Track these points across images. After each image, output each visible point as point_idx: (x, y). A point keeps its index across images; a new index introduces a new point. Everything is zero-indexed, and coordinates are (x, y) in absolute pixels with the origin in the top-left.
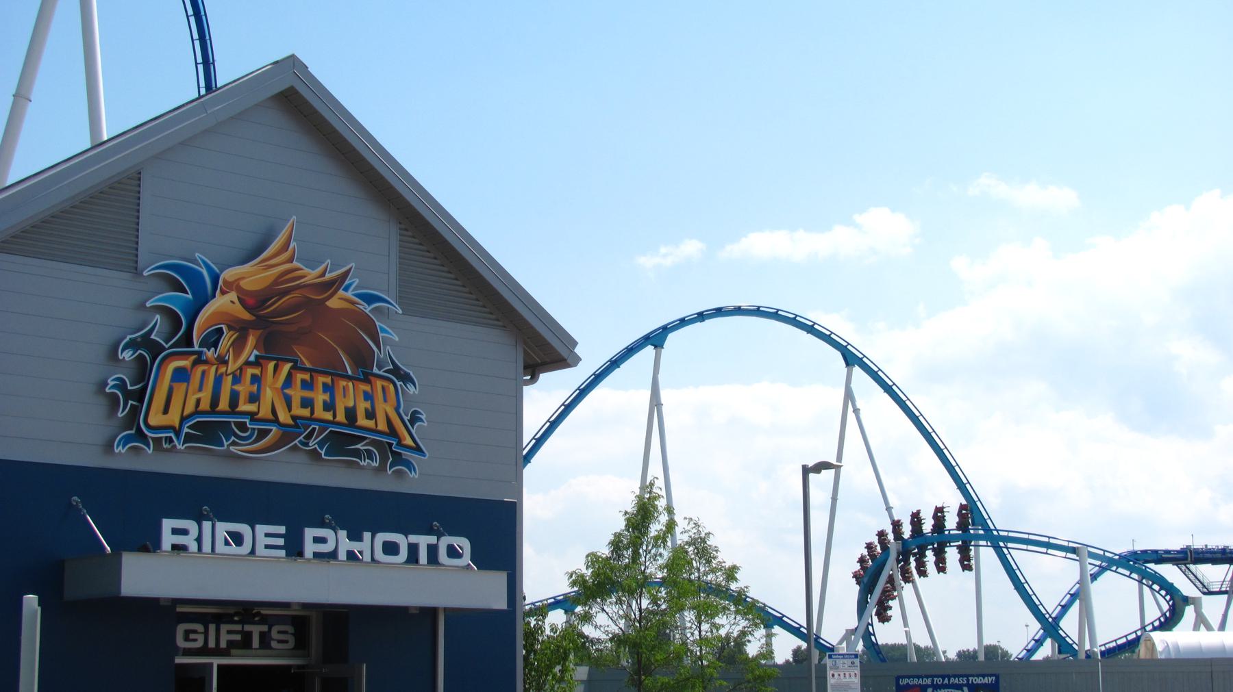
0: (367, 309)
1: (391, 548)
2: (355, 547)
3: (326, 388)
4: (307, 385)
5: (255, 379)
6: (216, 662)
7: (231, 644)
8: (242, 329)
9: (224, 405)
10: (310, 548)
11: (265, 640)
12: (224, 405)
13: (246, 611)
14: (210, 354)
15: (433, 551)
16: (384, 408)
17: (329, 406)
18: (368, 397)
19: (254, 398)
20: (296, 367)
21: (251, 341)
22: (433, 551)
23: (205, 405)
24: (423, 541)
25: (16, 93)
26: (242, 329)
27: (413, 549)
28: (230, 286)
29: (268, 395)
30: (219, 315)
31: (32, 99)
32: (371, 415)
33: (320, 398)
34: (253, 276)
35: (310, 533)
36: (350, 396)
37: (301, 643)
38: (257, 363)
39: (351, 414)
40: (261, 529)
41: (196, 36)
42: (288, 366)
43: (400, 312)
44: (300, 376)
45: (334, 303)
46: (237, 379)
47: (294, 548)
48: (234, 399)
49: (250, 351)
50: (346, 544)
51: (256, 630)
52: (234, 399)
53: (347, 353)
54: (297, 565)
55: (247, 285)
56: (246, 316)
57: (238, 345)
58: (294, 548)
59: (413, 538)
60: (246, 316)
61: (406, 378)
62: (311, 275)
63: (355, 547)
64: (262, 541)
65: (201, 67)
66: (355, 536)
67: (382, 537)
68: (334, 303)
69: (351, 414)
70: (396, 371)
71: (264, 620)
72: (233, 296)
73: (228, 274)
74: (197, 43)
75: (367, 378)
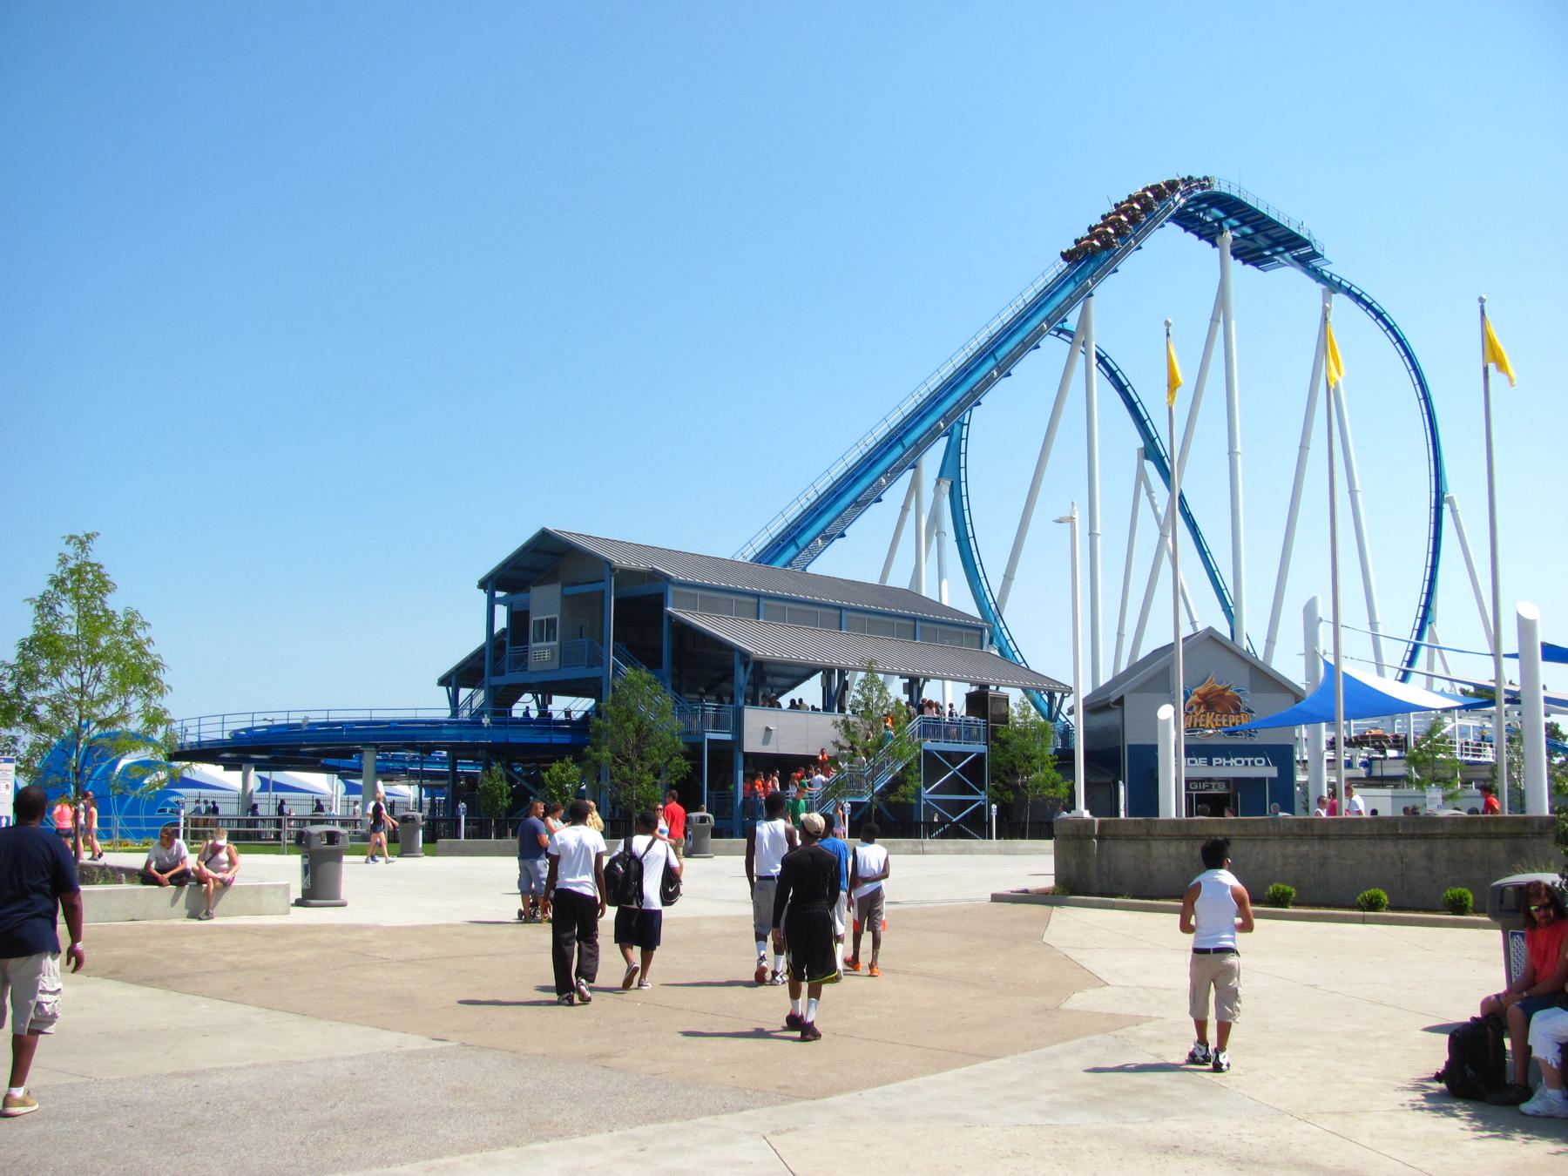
0: (1237, 694)
1: (1239, 762)
2: (1228, 762)
3: (1226, 718)
4: (1219, 717)
5: (1204, 718)
6: (1194, 793)
7: (1206, 788)
8: (1199, 705)
9: (1195, 725)
10: (1214, 763)
11: (1216, 786)
12: (1195, 725)
13: (1209, 780)
14: (1190, 712)
15: (1253, 763)
16: (1245, 722)
17: (1227, 723)
18: (1239, 719)
19: (1204, 723)
20: (1217, 713)
21: (1202, 707)
22: (1253, 763)
23: (1190, 726)
24: (1249, 760)
25: (1301, 444)
26: (1199, 705)
27: (1246, 763)
28: (1195, 693)
29: (1208, 721)
30: (1193, 702)
31: (1311, 446)
32: (1240, 723)
33: (1224, 721)
34: (1202, 690)
35: (1214, 759)
36: (1233, 719)
37: (1228, 787)
38: (1204, 713)
39: (1234, 724)
40: (1200, 759)
41: (1416, 382)
42: (1213, 714)
43: (1249, 692)
44: (1217, 716)
45: (1227, 694)
46: (1199, 717)
47: (1210, 763)
48: (1198, 724)
49: (1202, 710)
50: (1225, 761)
51: (1213, 784)
52: (1198, 724)
53: (1232, 707)
54: (1210, 768)
55: (1200, 692)
56: (1200, 701)
57: (1198, 709)
58: (1210, 763)
59: (1246, 759)
60: (1200, 701)
61: (1252, 712)
62: (1220, 687)
63: (1228, 762)
64: (1200, 762)
65: (1422, 401)
66: (1228, 759)
67: (1236, 759)
68: (1227, 694)
69: (1234, 724)
70: (1249, 711)
71: (1215, 781)
72: (1196, 696)
73: (1195, 690)
74: (1418, 387)
75: (1239, 714)
